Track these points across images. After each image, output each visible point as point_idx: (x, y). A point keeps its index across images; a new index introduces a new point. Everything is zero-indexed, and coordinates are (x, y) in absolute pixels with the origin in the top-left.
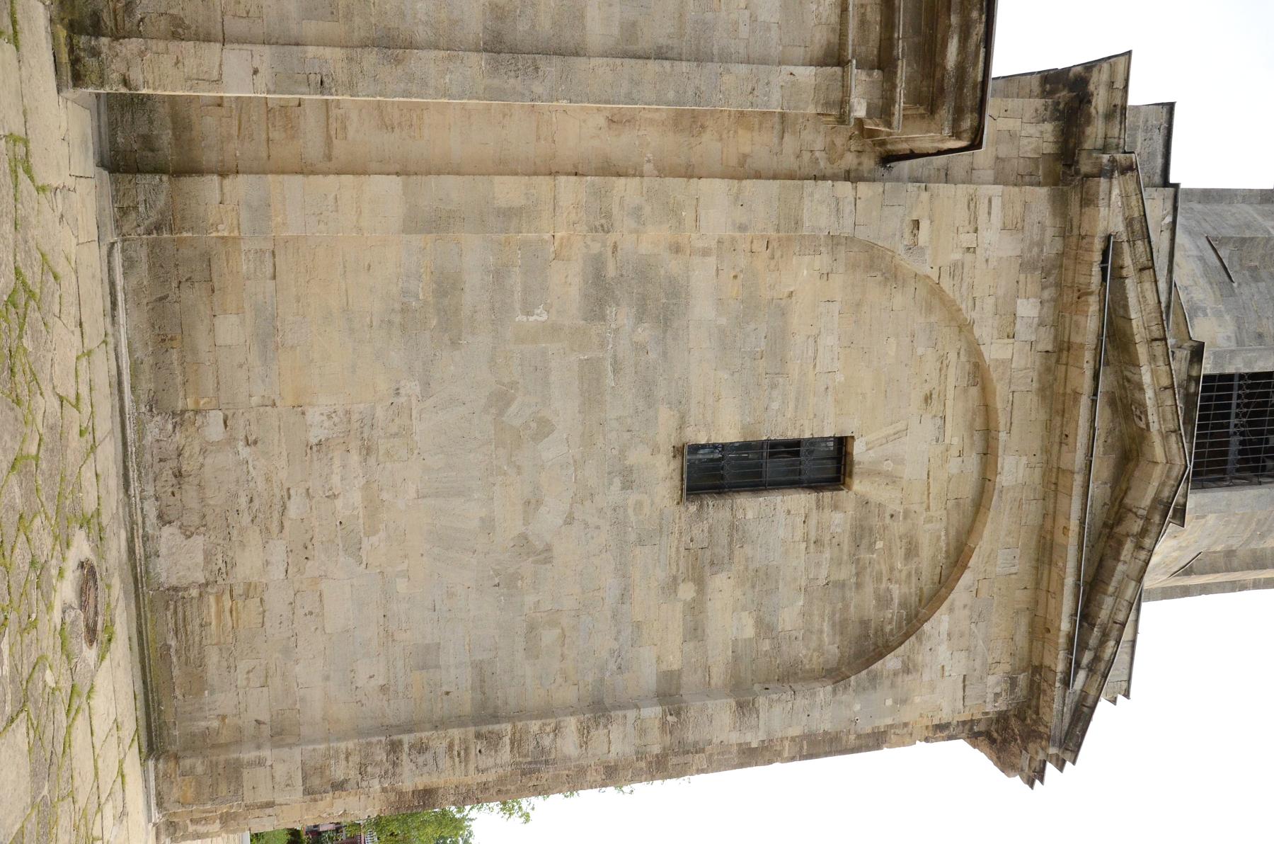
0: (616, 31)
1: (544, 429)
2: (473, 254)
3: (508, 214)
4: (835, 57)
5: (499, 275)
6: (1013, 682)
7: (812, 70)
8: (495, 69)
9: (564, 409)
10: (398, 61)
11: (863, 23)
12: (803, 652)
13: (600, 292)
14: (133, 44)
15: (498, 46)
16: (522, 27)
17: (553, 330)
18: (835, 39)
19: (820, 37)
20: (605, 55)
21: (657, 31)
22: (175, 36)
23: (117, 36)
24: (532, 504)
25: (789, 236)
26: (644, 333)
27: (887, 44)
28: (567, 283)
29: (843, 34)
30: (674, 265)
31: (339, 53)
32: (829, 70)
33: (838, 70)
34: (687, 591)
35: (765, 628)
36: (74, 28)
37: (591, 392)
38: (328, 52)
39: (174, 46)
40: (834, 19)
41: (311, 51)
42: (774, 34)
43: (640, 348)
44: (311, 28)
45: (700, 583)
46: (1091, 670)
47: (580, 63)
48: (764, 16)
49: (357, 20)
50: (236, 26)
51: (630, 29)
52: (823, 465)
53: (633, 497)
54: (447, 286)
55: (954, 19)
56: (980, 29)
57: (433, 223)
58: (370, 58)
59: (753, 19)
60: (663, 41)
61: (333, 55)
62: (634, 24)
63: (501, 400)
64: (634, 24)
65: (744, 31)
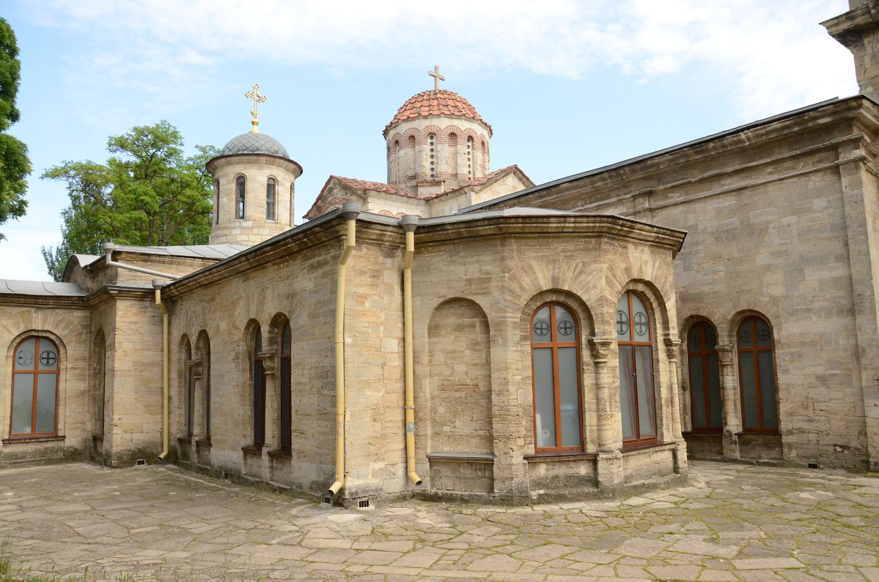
0: (840, 264)
4: (836, 170)
7: (843, 179)
8: (861, 312)
10: (864, 350)
11: (820, 161)
14: (870, 449)
15: (852, 312)
16: (844, 302)
18: (829, 172)
19: (829, 178)
20: (850, 268)
21: (836, 247)
22: (866, 434)
23: (869, 456)
27: (827, 149)
29: (826, 169)
31: (864, 374)
32: (841, 171)
33: (841, 168)
36: (868, 470)
38: (864, 378)
39: (869, 435)
40: (820, 174)
41: (864, 384)
42: (831, 198)
44: (856, 384)
47: (854, 277)
48: (824, 204)
49: (851, 366)
50: (859, 412)
51: (839, 258)
55: (810, 125)
56: (811, 113)
58: (864, 361)
59: (826, 208)
60: (841, 244)
61: (865, 375)
62: (836, 257)
64: (836, 257)
65: (832, 211)
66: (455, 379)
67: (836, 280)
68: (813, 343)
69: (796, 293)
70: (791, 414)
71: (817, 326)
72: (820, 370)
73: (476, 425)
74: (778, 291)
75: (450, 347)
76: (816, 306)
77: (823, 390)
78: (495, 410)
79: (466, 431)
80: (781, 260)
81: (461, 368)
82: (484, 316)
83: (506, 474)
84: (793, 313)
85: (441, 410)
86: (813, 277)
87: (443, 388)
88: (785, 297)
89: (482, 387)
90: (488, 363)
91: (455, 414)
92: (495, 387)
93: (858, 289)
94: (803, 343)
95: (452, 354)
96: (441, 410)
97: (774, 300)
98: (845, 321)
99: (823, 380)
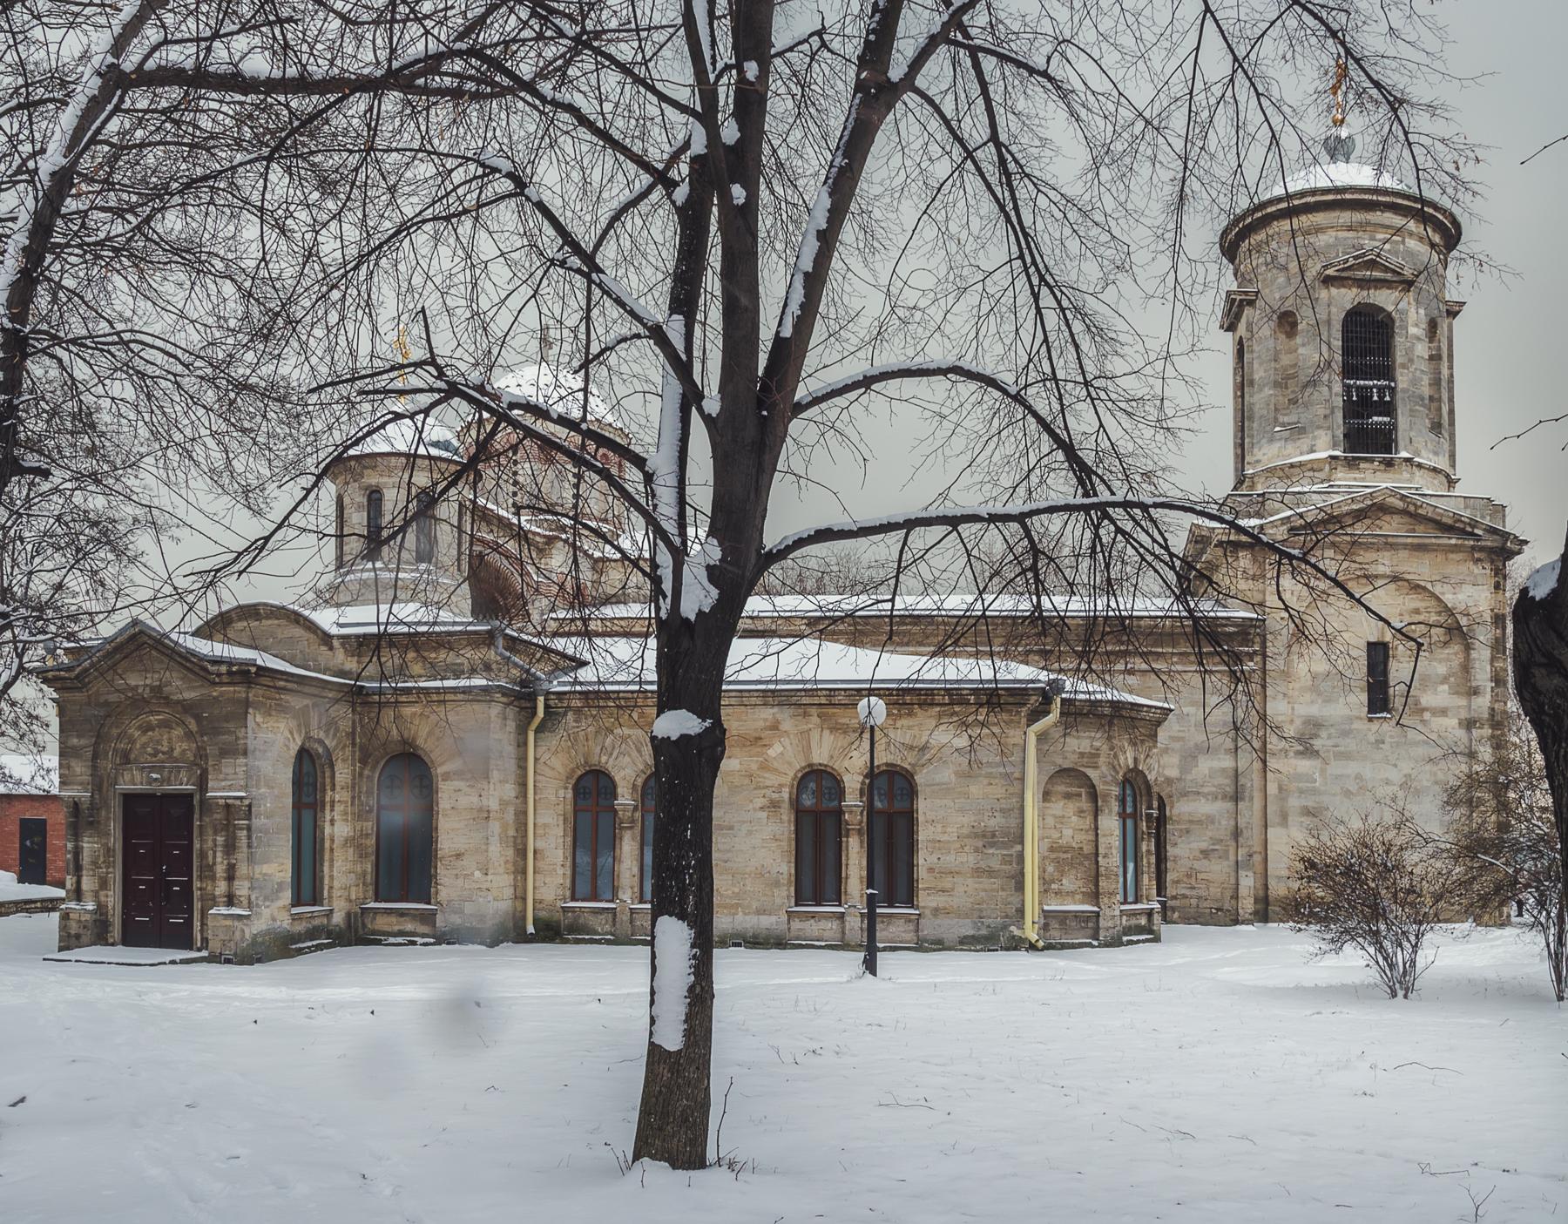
1: (1359, 777)
2: (1294, 802)
3: (1280, 788)
5: (1301, 792)
6: (1479, 560)
8: (1243, 799)
9: (1352, 768)
12: (1457, 661)
13: (1309, 751)
15: (1236, 797)
17: (1323, 771)
24: (1388, 782)
25: (1286, 675)
26: (1324, 734)
28: (1305, 765)
30: (1298, 722)
34: (1427, 715)
35: (1445, 680)
37: (1346, 756)
43: (1329, 737)
44: (1232, 858)
45: (1424, 710)
46: (1473, 527)
51: (1227, 751)
52: (1378, 654)
53: (1388, 740)
54: (1307, 812)
57: (1284, 818)
63: (1348, 794)
66: (1063, 842)
67: (1224, 770)
68: (1200, 822)
69: (1189, 777)
70: (1178, 882)
71: (1203, 807)
72: (1204, 845)
73: (1080, 883)
74: (1173, 773)
75: (1059, 813)
76: (1206, 790)
77: (1206, 862)
78: (1102, 870)
79: (1072, 888)
80: (1177, 745)
81: (1068, 832)
82: (1093, 786)
83: (1110, 924)
84: (1185, 794)
85: (1050, 869)
86: (1205, 765)
87: (1052, 849)
88: (1179, 780)
89: (1088, 849)
90: (1097, 828)
91: (1062, 873)
92: (1101, 850)
93: (1242, 781)
94: (1191, 822)
95: (1061, 819)
96: (1050, 869)
97: (1169, 781)
98: (1230, 805)
99: (1206, 854)
